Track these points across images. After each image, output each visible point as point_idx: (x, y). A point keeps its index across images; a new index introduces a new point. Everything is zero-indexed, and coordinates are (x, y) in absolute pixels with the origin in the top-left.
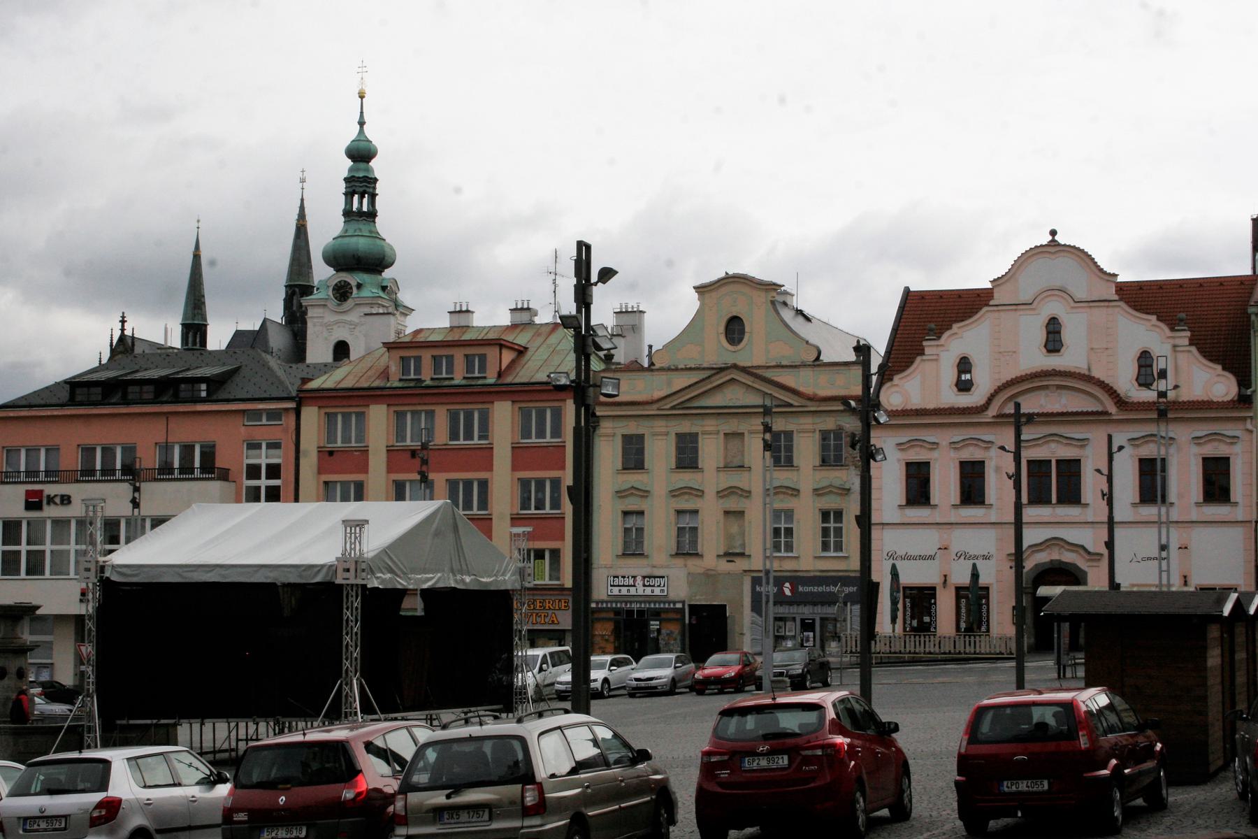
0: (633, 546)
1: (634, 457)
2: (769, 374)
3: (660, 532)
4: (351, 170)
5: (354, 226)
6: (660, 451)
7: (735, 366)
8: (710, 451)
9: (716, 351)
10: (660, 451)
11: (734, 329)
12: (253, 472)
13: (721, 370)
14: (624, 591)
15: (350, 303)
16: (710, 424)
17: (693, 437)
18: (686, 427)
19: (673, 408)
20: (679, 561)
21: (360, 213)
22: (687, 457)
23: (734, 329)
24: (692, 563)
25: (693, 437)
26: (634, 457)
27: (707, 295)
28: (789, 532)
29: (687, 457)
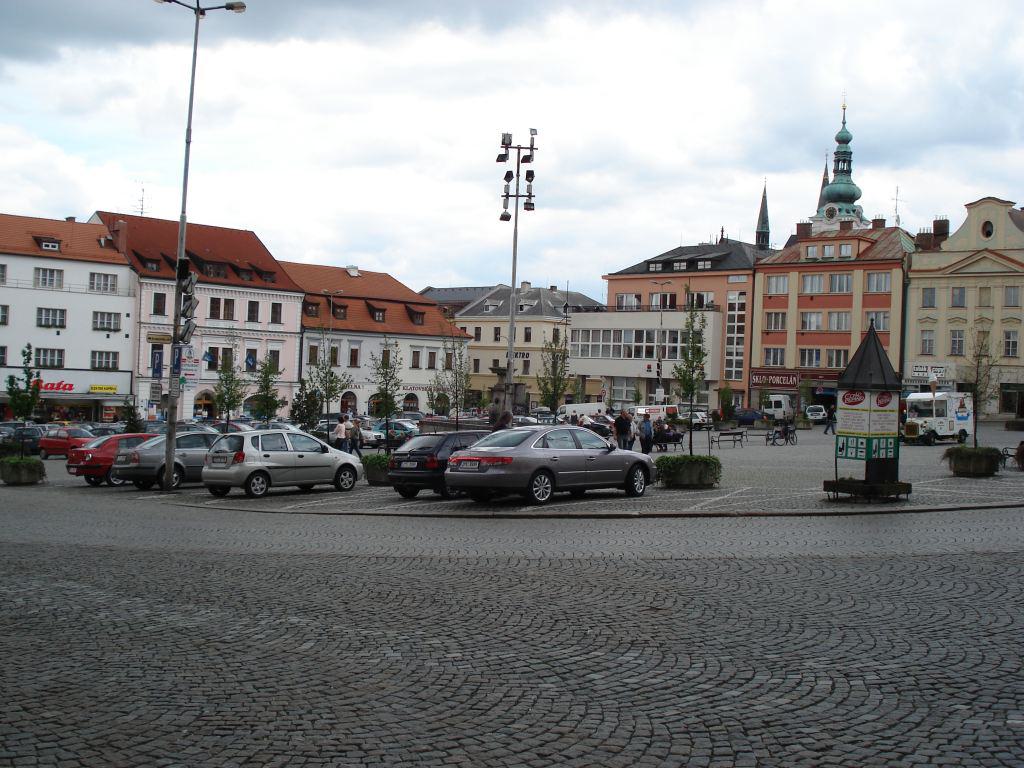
0: (927, 351)
1: (929, 302)
2: (1005, 254)
3: (942, 344)
4: (838, 147)
5: (839, 177)
6: (943, 298)
7: (986, 250)
8: (971, 297)
9: (978, 241)
10: (943, 298)
11: (988, 230)
12: (732, 307)
13: (979, 252)
14: (921, 374)
15: (835, 219)
16: (971, 282)
17: (933, 290)
18: (958, 283)
19: (951, 273)
20: (953, 358)
21: (843, 171)
22: (958, 303)
23: (988, 230)
24: (959, 359)
25: (933, 290)
26: (929, 302)
27: (972, 210)
28: (1015, 344)
29: (958, 303)
